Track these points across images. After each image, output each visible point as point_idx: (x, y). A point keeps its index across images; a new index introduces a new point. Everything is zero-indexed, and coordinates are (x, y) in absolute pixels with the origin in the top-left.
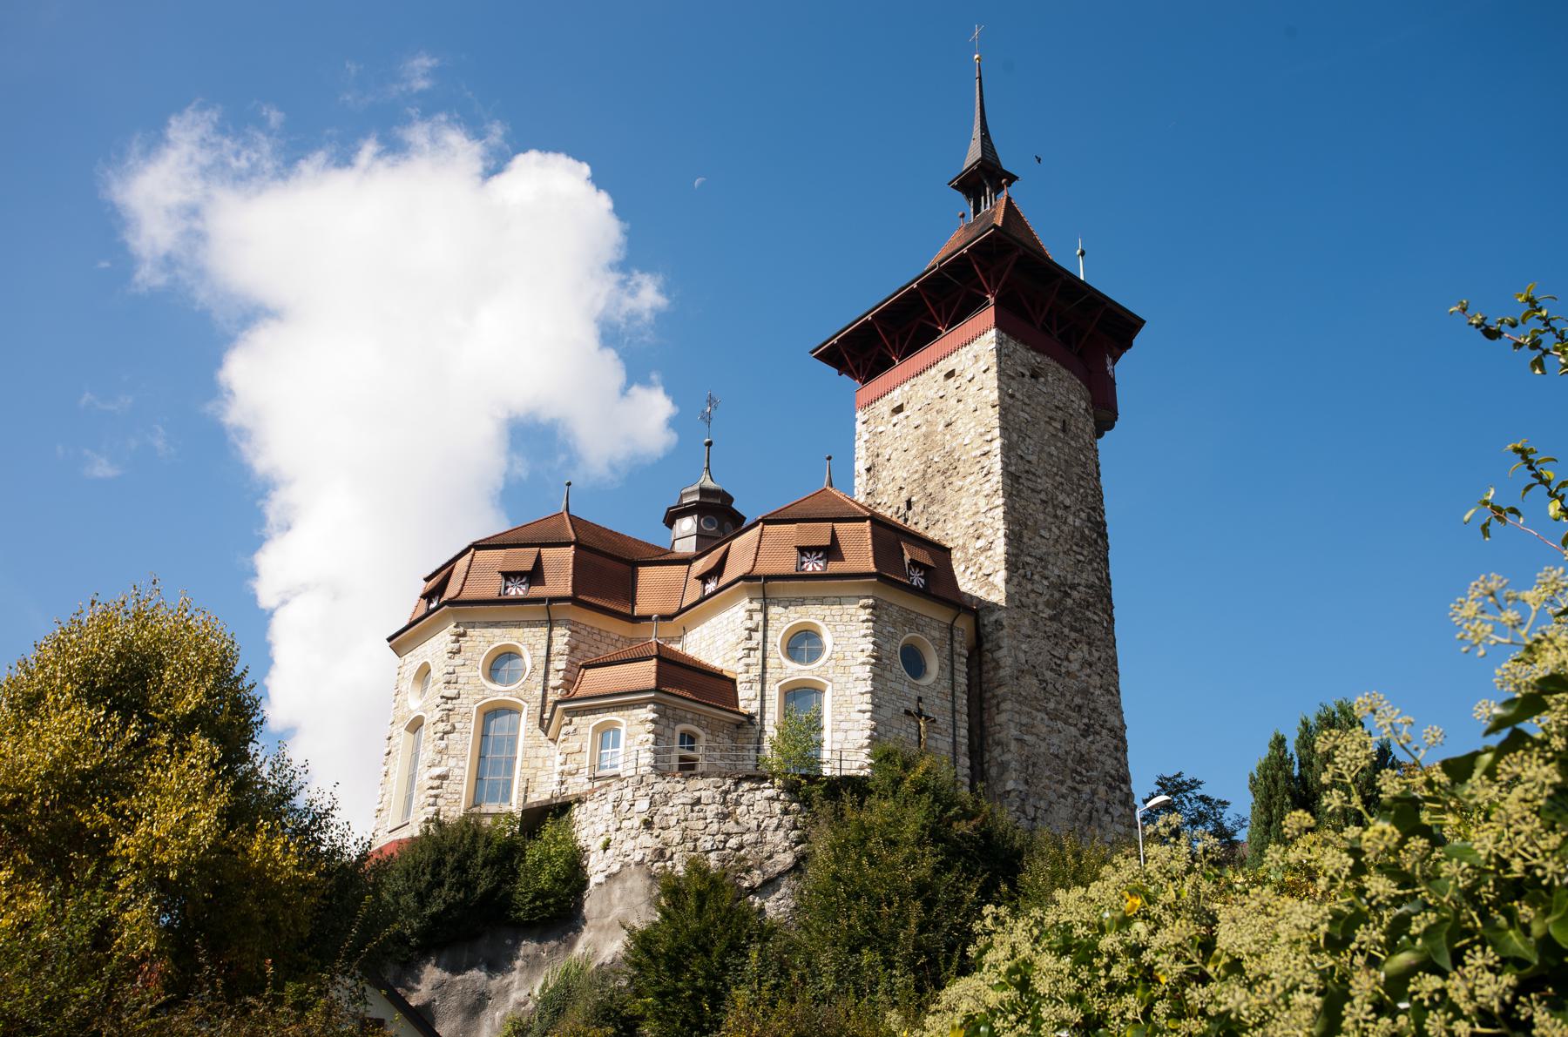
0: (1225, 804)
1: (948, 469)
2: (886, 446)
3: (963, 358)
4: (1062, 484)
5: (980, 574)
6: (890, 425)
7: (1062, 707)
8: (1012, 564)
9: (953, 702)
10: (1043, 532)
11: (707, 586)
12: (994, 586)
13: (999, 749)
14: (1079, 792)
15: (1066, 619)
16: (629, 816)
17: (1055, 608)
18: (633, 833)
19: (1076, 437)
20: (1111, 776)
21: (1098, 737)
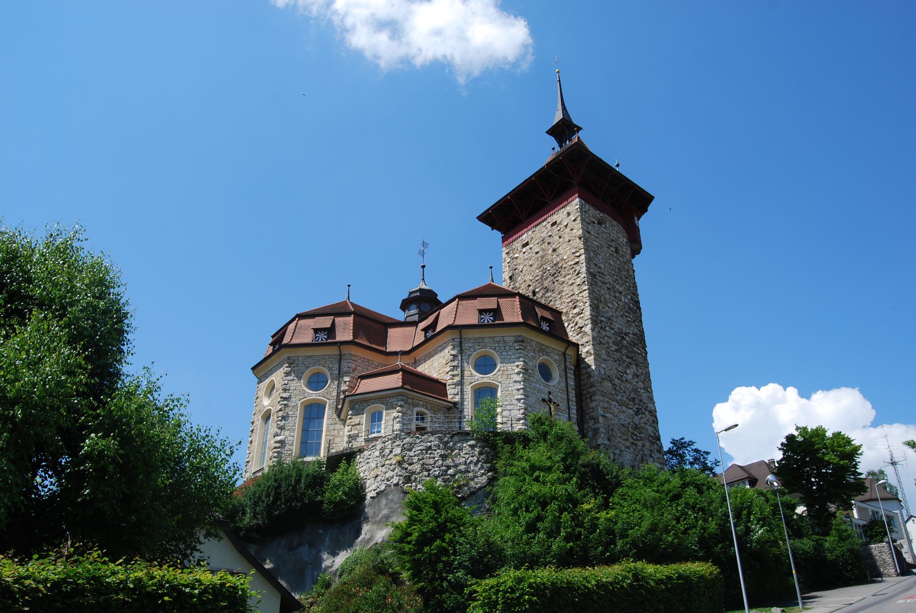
0: (708, 453)
1: (555, 273)
2: (520, 264)
3: (561, 214)
4: (617, 280)
5: (577, 327)
6: (522, 253)
7: (625, 399)
8: (595, 321)
9: (568, 395)
10: (609, 305)
11: (428, 334)
12: (585, 333)
13: (593, 421)
14: (636, 445)
15: (624, 351)
16: (389, 457)
17: (618, 345)
18: (392, 468)
19: (622, 256)
20: (652, 437)
21: (644, 415)
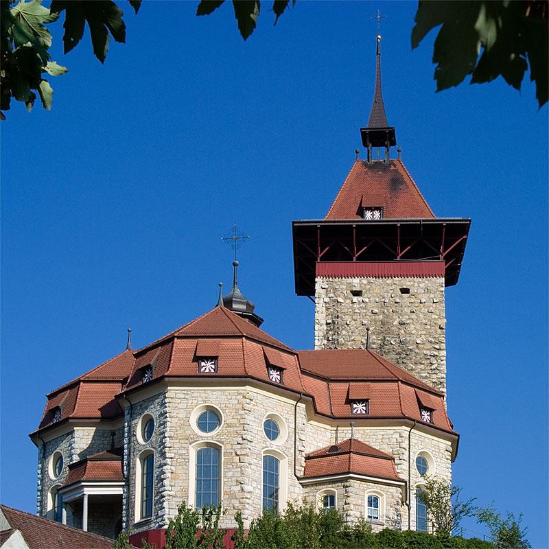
2: (345, 314)
